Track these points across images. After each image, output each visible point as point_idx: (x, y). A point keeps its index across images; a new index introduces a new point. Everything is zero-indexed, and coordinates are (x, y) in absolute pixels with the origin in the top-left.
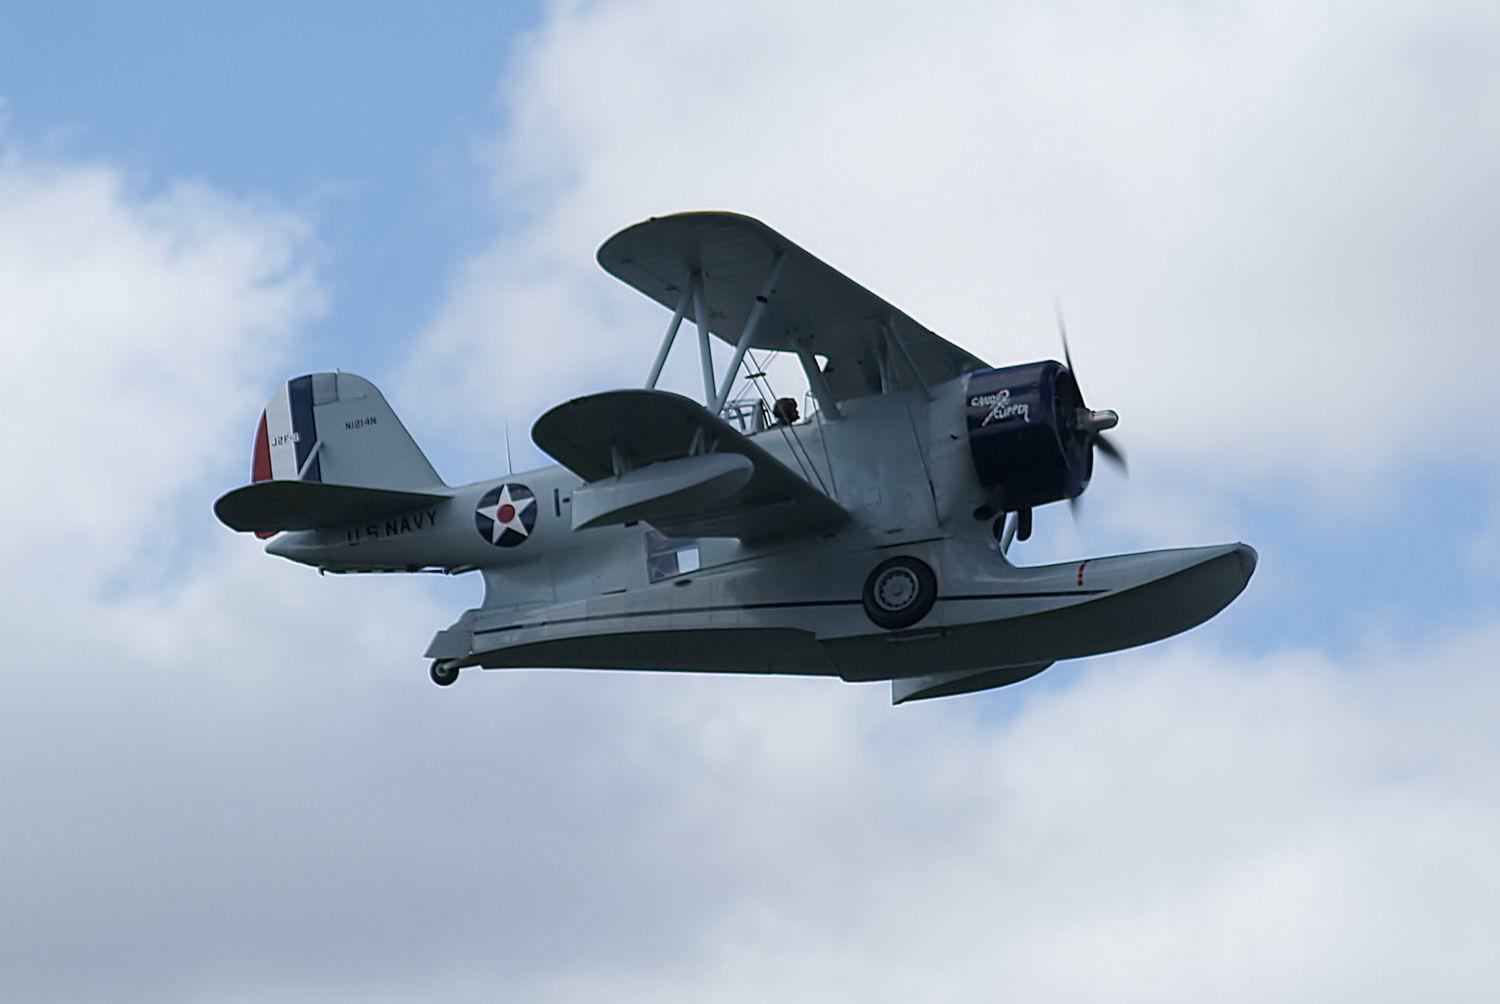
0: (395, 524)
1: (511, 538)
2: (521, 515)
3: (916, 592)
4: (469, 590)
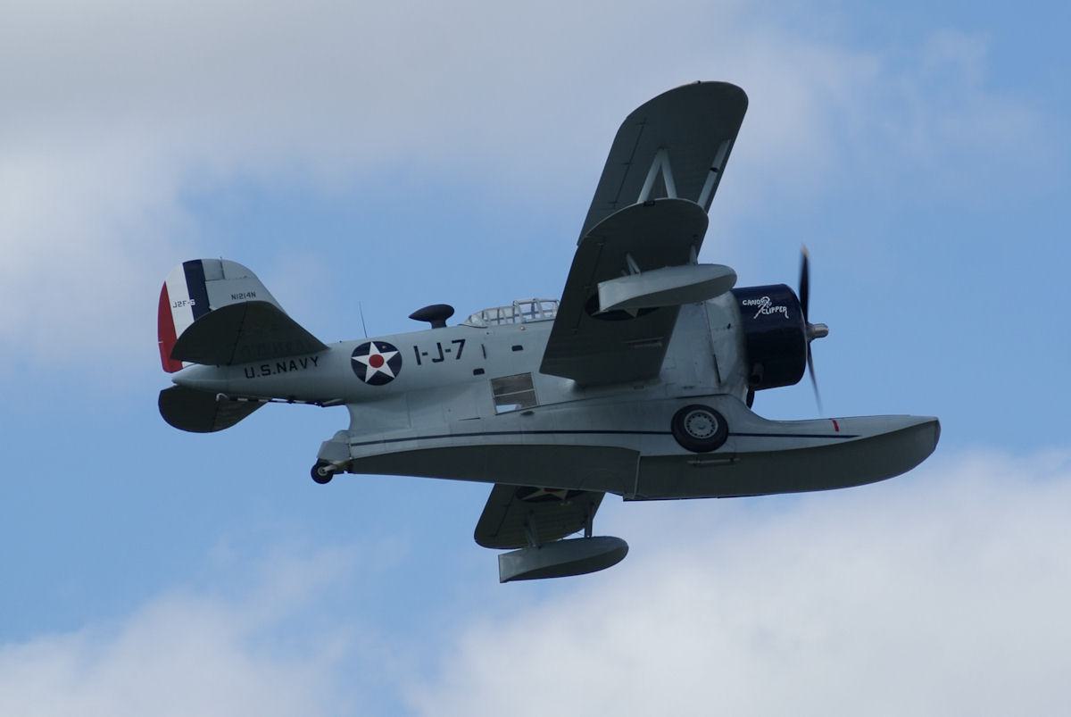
0: (284, 364)
1: (380, 379)
2: (388, 363)
3: (713, 434)
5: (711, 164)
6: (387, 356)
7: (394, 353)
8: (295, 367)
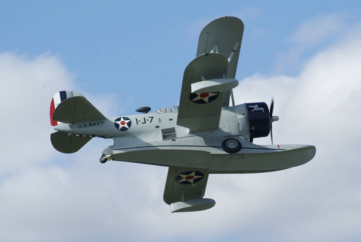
1: (124, 129)
4: (110, 142)
5: (234, 54)
6: (127, 122)
7: (128, 121)
8: (95, 125)
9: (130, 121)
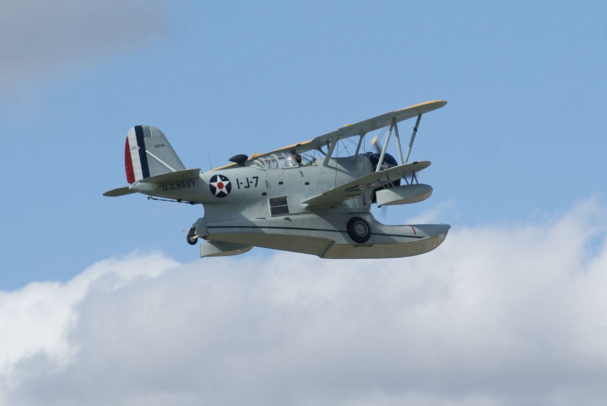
1: (222, 195)
6: (225, 183)
9: (230, 183)
